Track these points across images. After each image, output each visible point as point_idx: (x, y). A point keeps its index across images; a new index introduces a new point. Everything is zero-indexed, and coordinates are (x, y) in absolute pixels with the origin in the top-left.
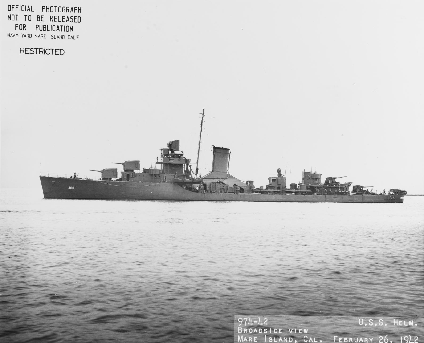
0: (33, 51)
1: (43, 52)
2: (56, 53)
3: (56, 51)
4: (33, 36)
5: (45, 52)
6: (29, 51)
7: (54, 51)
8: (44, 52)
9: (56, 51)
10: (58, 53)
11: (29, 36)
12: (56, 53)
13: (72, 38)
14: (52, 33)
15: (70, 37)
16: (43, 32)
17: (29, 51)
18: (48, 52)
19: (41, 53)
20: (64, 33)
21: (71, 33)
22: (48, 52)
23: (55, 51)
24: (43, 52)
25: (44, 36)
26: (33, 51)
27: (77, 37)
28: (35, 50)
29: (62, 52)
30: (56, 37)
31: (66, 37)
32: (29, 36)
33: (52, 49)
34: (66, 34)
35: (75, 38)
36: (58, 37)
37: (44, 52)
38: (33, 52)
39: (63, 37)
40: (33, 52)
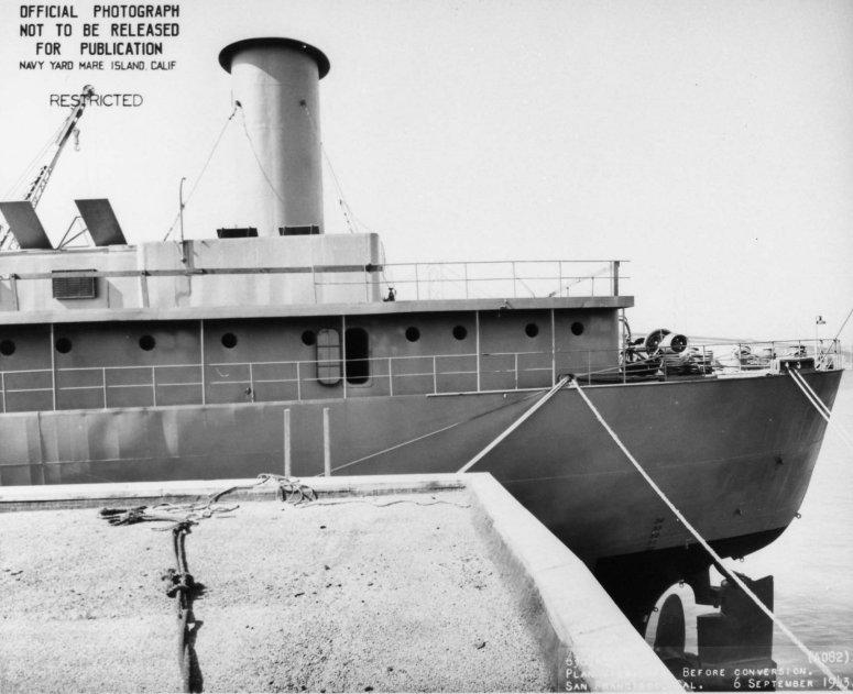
2: (126, 103)
4: (76, 65)
5: (103, 101)
7: (121, 98)
10: (130, 100)
11: (66, 65)
12: (126, 103)
13: (160, 66)
14: (117, 57)
15: (155, 66)
16: (97, 58)
18: (108, 100)
21: (158, 57)
22: (108, 100)
23: (124, 100)
25: (99, 65)
27: (172, 64)
29: (138, 100)
30: (125, 66)
31: (148, 65)
32: (66, 65)
34: (148, 59)
35: (166, 66)
39: (139, 66)
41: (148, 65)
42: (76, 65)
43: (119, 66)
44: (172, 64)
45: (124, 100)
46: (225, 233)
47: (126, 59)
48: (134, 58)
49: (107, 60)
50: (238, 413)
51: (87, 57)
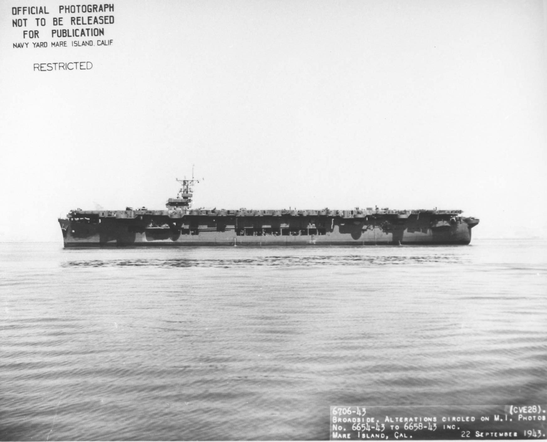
0: (51, 66)
1: (65, 67)
3: (82, 64)
4: (49, 44)
5: (67, 67)
6: (45, 67)
7: (78, 65)
8: (66, 66)
9: (82, 64)
13: (103, 43)
14: (75, 39)
15: (100, 43)
16: (62, 39)
17: (45, 67)
18: (70, 66)
19: (61, 68)
20: (90, 38)
21: (101, 38)
22: (70, 66)
23: (80, 65)
24: (65, 67)
25: (64, 44)
26: (51, 66)
27: (110, 42)
28: (53, 66)
29: (89, 65)
30: (81, 44)
31: (95, 43)
33: (76, 63)
34: (95, 39)
35: (107, 43)
36: (84, 44)
37: (66, 66)
38: (51, 68)
39: (90, 43)
40: (51, 68)
41: (95, 43)
42: (49, 44)
43: (76, 44)
44: (110, 42)
45: (80, 65)
46: (88, 230)
47: (81, 39)
48: (86, 39)
49: (69, 40)
50: (166, 238)
51: (56, 39)
